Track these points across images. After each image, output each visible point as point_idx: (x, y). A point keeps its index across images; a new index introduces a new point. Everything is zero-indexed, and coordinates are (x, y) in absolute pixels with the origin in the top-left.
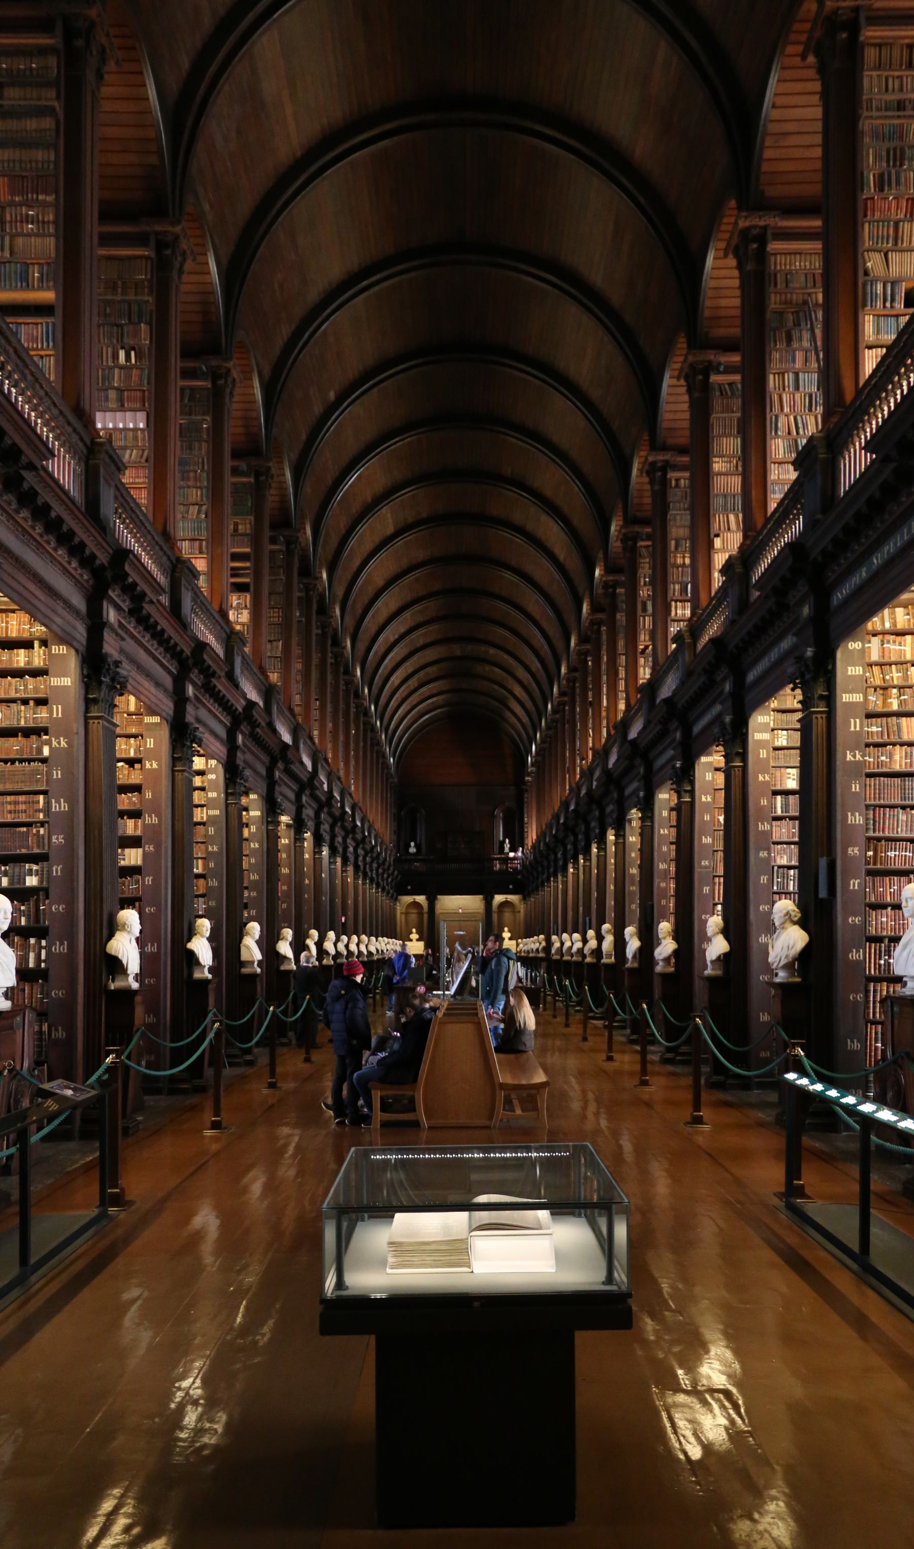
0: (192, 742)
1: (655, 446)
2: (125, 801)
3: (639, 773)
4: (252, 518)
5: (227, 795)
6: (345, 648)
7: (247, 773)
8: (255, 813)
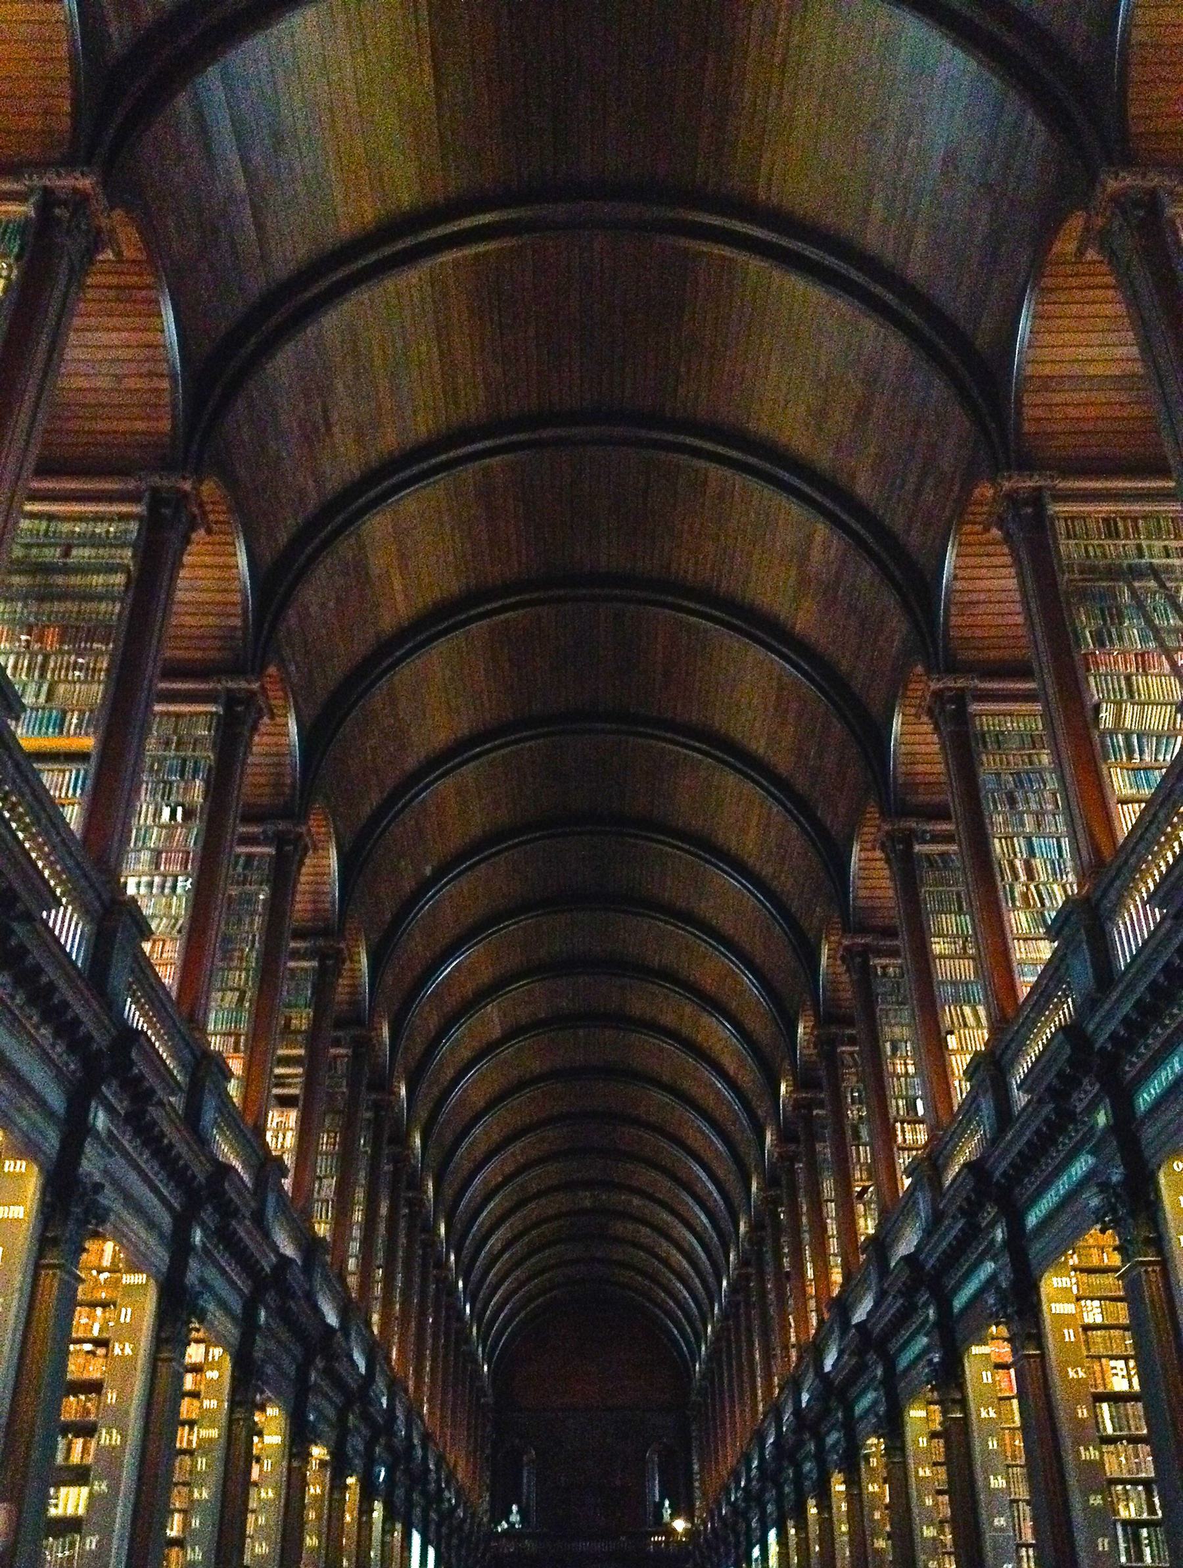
2: (71, 1408)
3: (875, 1377)
5: (233, 1404)
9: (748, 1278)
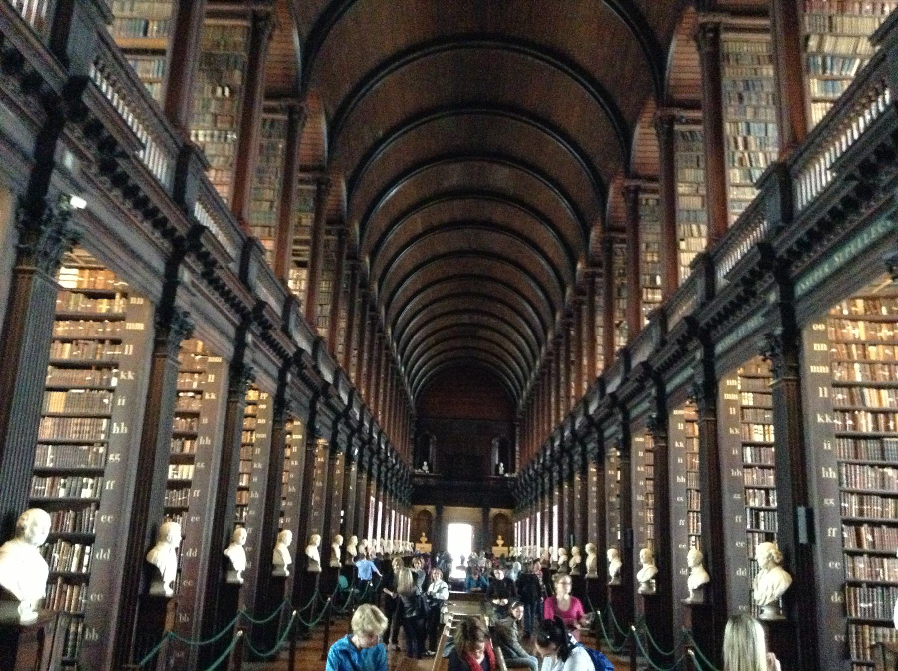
0: (247, 379)
1: (629, 174)
4: (313, 215)
5: (275, 422)
6: (380, 312)
7: (293, 405)
8: (298, 437)
9: (550, 362)
